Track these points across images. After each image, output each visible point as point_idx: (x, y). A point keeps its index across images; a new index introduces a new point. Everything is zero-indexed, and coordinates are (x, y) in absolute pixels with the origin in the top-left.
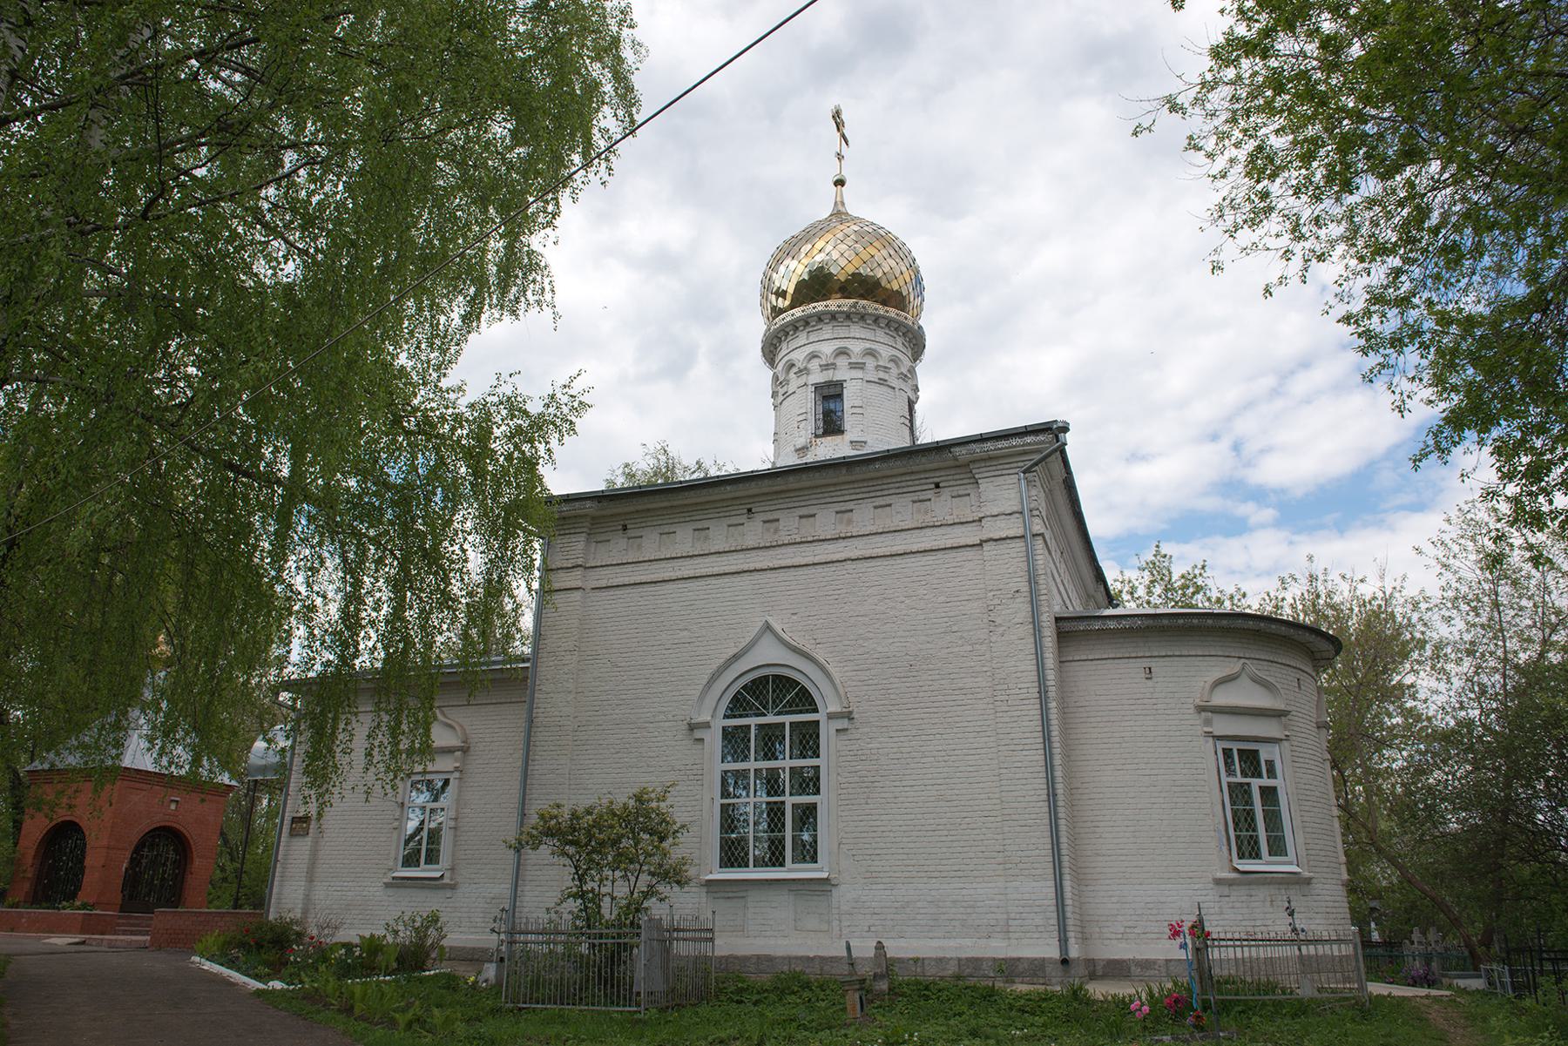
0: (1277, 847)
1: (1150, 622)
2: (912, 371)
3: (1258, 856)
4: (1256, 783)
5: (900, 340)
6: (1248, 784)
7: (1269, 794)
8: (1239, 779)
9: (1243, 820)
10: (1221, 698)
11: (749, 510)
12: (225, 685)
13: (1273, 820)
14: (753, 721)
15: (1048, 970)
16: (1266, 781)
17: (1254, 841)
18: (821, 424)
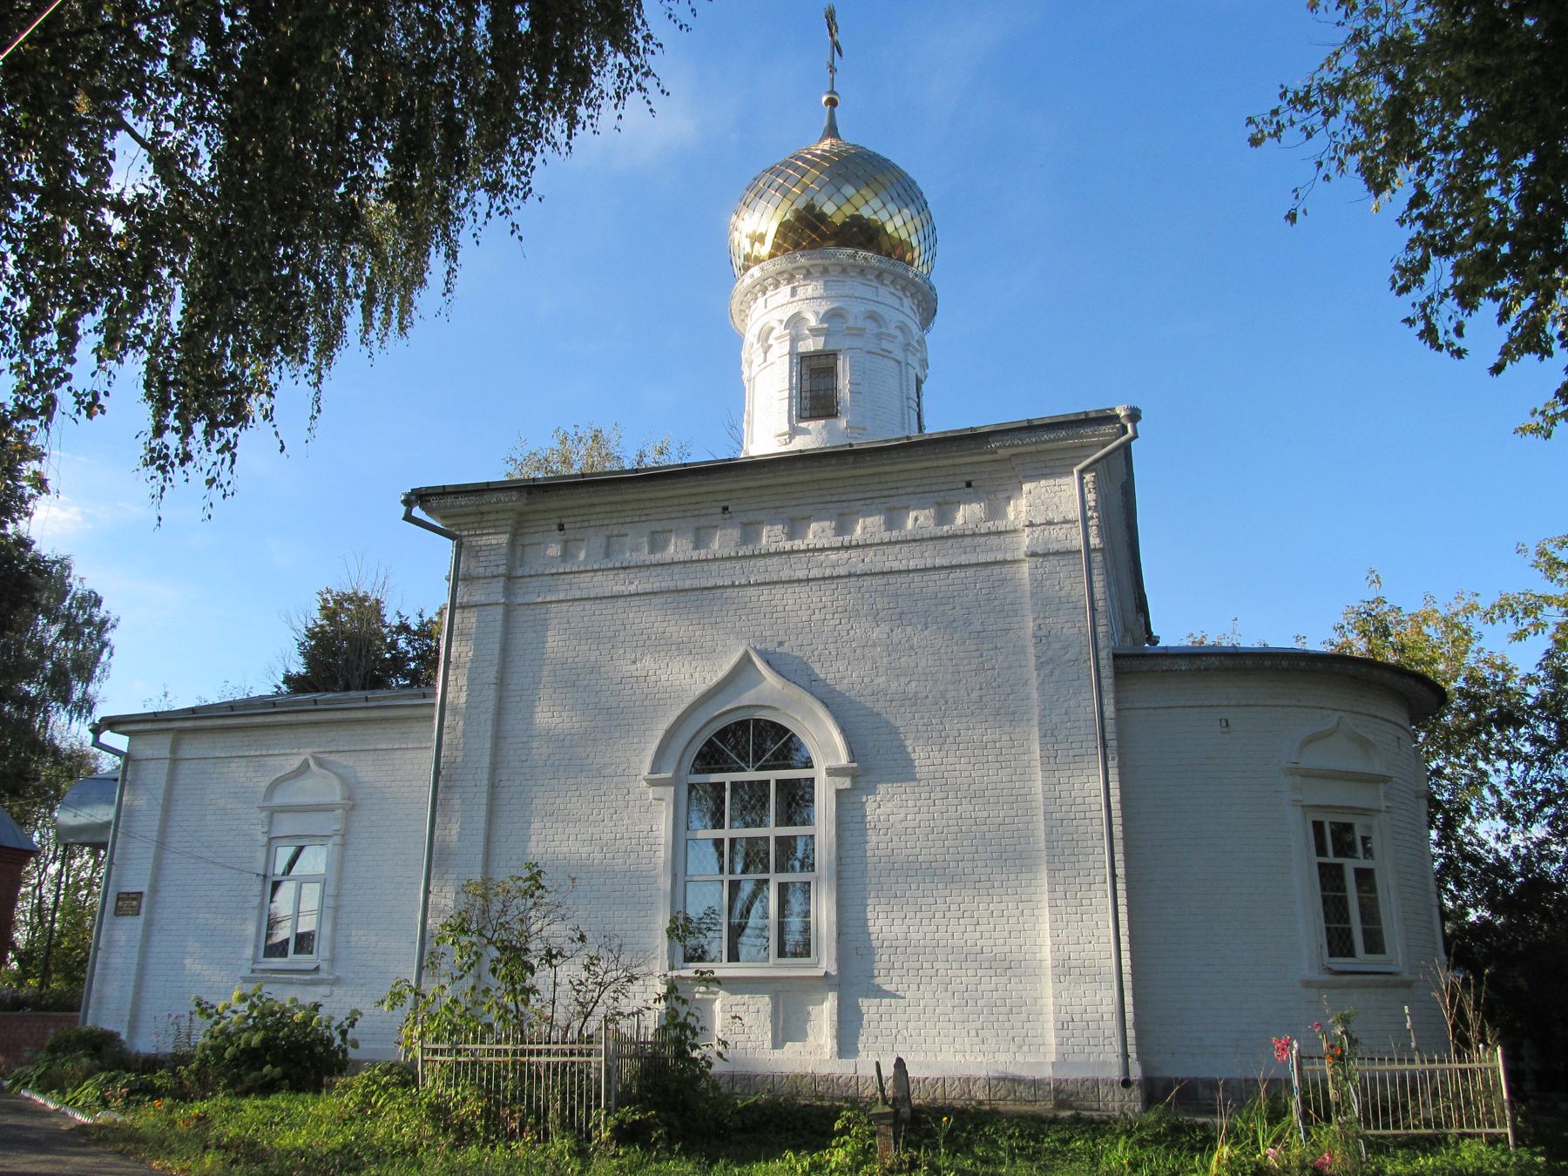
0: (1374, 944)
1: (1229, 662)
2: (921, 342)
3: (1350, 953)
4: (1350, 865)
5: (907, 302)
6: (1340, 866)
7: (1364, 876)
8: (1331, 859)
9: (1334, 908)
10: (1315, 759)
11: (725, 509)
12: (520, 459)
13: (1370, 914)
14: (727, 778)
15: (1103, 1091)
16: (1363, 863)
17: (1347, 934)
18: (807, 403)
